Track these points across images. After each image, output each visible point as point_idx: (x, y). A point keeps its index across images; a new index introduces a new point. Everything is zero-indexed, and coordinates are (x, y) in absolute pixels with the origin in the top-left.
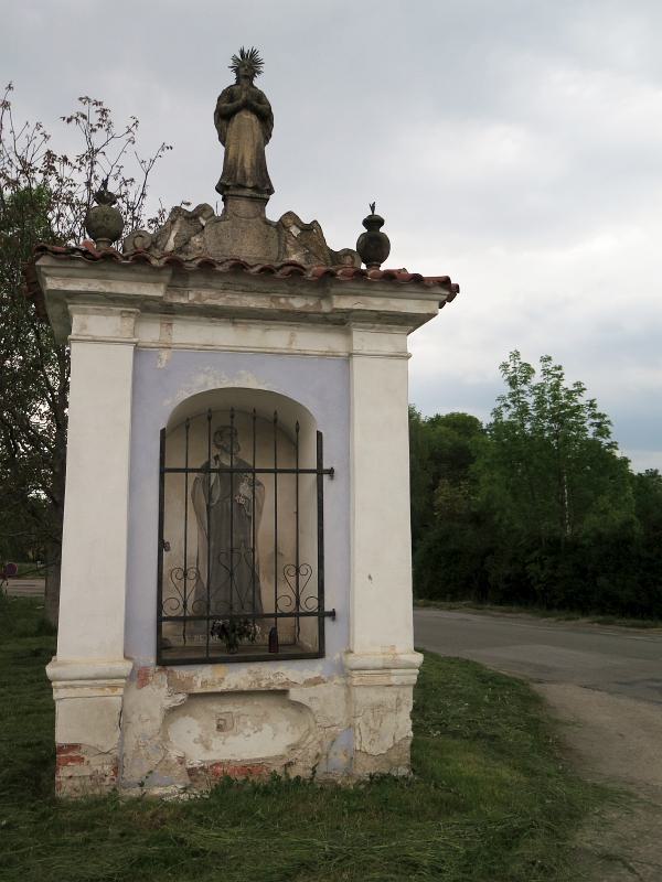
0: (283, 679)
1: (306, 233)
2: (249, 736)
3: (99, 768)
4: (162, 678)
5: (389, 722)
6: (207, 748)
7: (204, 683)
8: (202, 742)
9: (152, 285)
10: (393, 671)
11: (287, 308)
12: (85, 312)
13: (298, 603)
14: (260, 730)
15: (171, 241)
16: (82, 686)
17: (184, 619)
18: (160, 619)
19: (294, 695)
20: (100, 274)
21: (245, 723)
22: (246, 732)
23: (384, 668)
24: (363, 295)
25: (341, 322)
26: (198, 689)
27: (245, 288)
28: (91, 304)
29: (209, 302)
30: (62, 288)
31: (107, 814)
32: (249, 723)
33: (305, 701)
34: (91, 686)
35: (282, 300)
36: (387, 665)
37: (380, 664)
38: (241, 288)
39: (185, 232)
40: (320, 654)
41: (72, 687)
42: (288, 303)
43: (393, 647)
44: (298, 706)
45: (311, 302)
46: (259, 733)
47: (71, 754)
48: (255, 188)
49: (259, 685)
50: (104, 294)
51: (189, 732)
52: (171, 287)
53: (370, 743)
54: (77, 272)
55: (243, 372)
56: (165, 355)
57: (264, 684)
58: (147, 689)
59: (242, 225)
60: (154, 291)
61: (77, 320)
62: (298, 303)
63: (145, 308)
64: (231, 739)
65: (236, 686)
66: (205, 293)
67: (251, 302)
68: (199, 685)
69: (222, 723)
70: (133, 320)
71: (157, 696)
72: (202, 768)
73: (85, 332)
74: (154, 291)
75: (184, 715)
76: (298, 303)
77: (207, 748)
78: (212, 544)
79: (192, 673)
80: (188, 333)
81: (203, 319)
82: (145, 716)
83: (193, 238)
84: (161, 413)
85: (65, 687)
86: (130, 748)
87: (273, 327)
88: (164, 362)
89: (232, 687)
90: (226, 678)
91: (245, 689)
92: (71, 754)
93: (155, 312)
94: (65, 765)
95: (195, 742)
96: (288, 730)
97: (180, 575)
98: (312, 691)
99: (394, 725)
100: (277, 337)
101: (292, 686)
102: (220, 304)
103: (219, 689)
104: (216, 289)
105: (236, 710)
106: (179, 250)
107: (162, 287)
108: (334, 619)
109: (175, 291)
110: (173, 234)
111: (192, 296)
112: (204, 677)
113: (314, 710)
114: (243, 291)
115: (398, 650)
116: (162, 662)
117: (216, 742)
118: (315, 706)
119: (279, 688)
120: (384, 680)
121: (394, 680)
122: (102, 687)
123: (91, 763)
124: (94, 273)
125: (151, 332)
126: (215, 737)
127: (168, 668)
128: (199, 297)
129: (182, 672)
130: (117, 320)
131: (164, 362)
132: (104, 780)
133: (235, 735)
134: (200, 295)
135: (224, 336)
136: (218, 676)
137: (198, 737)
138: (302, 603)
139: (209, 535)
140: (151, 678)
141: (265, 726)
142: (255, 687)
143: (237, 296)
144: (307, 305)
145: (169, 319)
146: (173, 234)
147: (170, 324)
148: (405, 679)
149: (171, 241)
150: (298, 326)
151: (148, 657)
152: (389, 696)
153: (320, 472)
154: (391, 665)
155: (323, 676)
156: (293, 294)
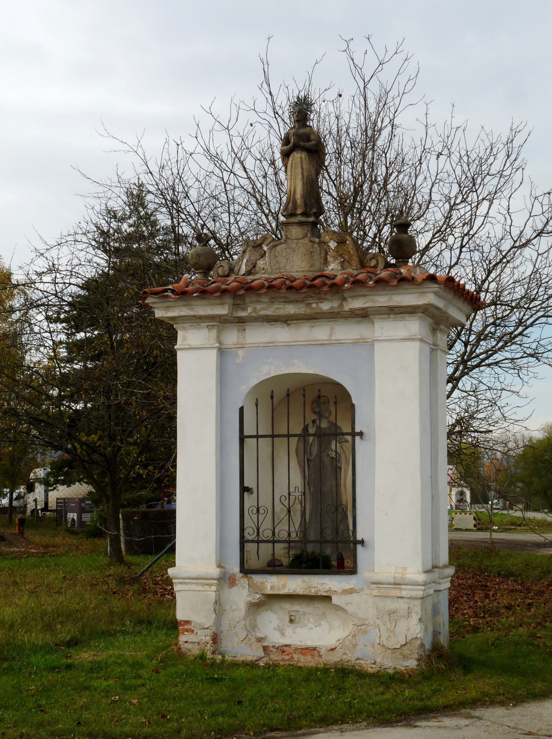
0: (327, 588)
1: (341, 245)
2: (311, 629)
3: (203, 638)
4: (244, 581)
5: (402, 626)
6: (283, 634)
7: (272, 588)
8: (279, 630)
9: (220, 306)
10: (403, 587)
11: (318, 311)
12: (184, 329)
13: (258, 533)
14: (320, 625)
15: (244, 267)
16: (191, 583)
17: (289, 542)
18: (243, 541)
19: (335, 600)
20: (185, 303)
21: (309, 619)
22: (310, 626)
23: (396, 584)
24: (370, 295)
25: (363, 315)
26: (269, 591)
27: (285, 300)
28: (188, 323)
29: (262, 313)
30: (165, 315)
31: (213, 669)
32: (311, 620)
33: (343, 605)
34: (196, 584)
35: (314, 306)
36: (397, 581)
37: (392, 580)
38: (283, 300)
39: (252, 258)
40: (353, 571)
41: (184, 583)
42: (318, 307)
43: (405, 569)
44: (338, 608)
45: (336, 304)
46: (318, 627)
47: (186, 627)
48: (303, 214)
49: (310, 591)
50: (194, 316)
51: (270, 622)
52: (236, 306)
53: (387, 639)
54: (171, 304)
55: (295, 361)
56: (241, 353)
57: (313, 591)
58: (235, 589)
59: (294, 246)
60: (222, 310)
61: (180, 335)
62: (325, 306)
63: (221, 322)
64: (298, 630)
65: (295, 591)
66: (259, 307)
67: (291, 309)
68: (269, 588)
69: (293, 618)
70: (215, 331)
71: (240, 596)
72: (273, 647)
73: (185, 343)
74: (222, 310)
75: (267, 610)
76: (325, 306)
77: (283, 634)
78: (312, 489)
79: (264, 580)
80: (257, 335)
81: (265, 323)
82: (234, 607)
83: (258, 262)
84: (240, 393)
85: (181, 583)
86: (225, 627)
87: (316, 324)
88: (240, 358)
89: (291, 592)
90: (287, 585)
91: (301, 593)
92: (186, 627)
93: (232, 323)
94: (183, 634)
95: (274, 629)
96: (339, 627)
97: (255, 511)
98: (348, 598)
99: (406, 628)
100: (321, 332)
101: (334, 594)
102: (270, 313)
103: (282, 592)
104: (264, 303)
105: (302, 610)
106: (249, 273)
107: (227, 307)
108: (363, 546)
109: (239, 307)
110: (245, 261)
111: (250, 310)
112: (274, 583)
113: (349, 612)
114: (284, 302)
115: (409, 570)
116: (245, 571)
117: (289, 630)
118: (351, 609)
119: (325, 594)
120: (397, 593)
121: (404, 593)
122: (204, 585)
123: (198, 634)
124: (182, 303)
125: (231, 337)
126: (288, 627)
127: (249, 576)
128: (255, 310)
129: (258, 579)
130: (206, 331)
131: (240, 358)
132: (206, 646)
133: (302, 627)
134: (256, 308)
135: (281, 334)
136: (282, 583)
137: (276, 626)
138: (261, 534)
139: (307, 482)
140: (237, 582)
141: (323, 622)
142: (306, 593)
143: (281, 306)
144: (332, 307)
145: (242, 326)
146: (245, 261)
147: (244, 330)
148: (414, 594)
149: (244, 267)
150: (336, 321)
151: (234, 567)
152: (402, 605)
153: (354, 434)
154: (401, 582)
155: (356, 588)
156: (321, 300)
